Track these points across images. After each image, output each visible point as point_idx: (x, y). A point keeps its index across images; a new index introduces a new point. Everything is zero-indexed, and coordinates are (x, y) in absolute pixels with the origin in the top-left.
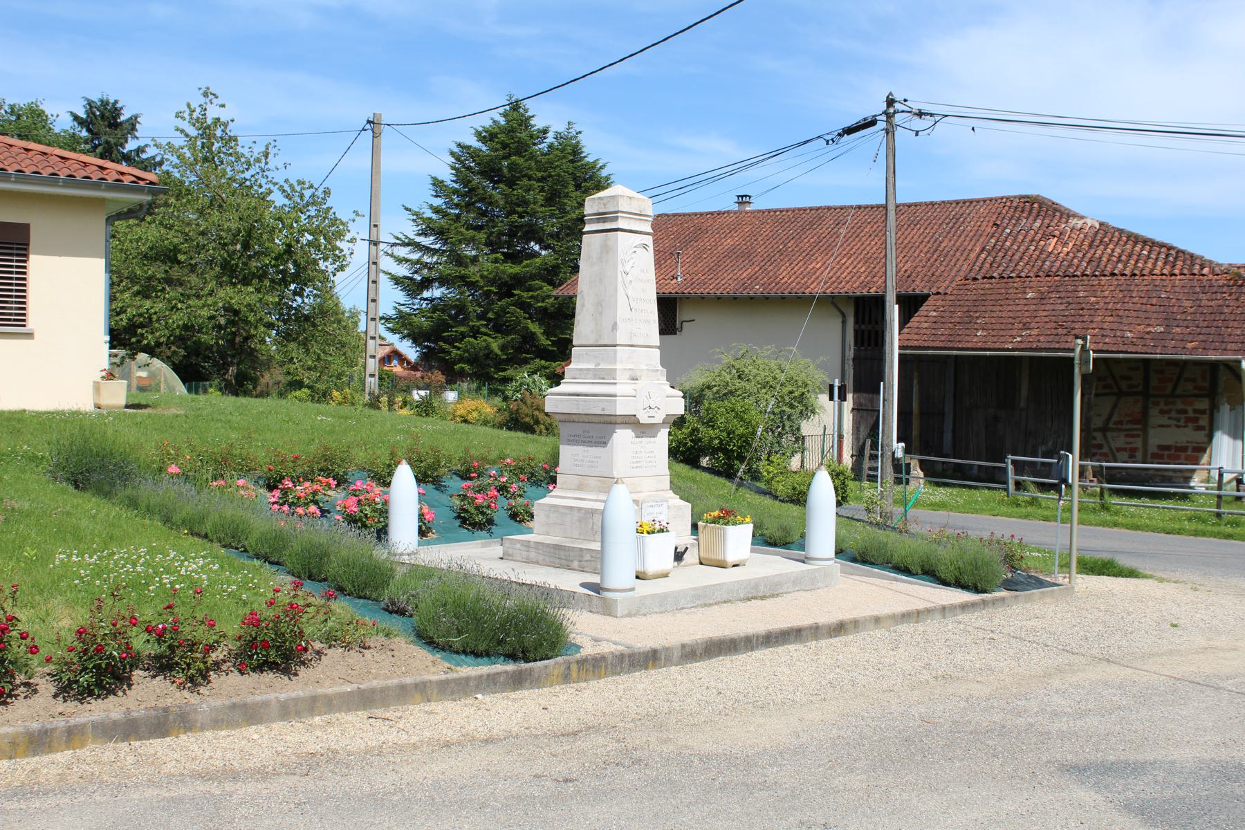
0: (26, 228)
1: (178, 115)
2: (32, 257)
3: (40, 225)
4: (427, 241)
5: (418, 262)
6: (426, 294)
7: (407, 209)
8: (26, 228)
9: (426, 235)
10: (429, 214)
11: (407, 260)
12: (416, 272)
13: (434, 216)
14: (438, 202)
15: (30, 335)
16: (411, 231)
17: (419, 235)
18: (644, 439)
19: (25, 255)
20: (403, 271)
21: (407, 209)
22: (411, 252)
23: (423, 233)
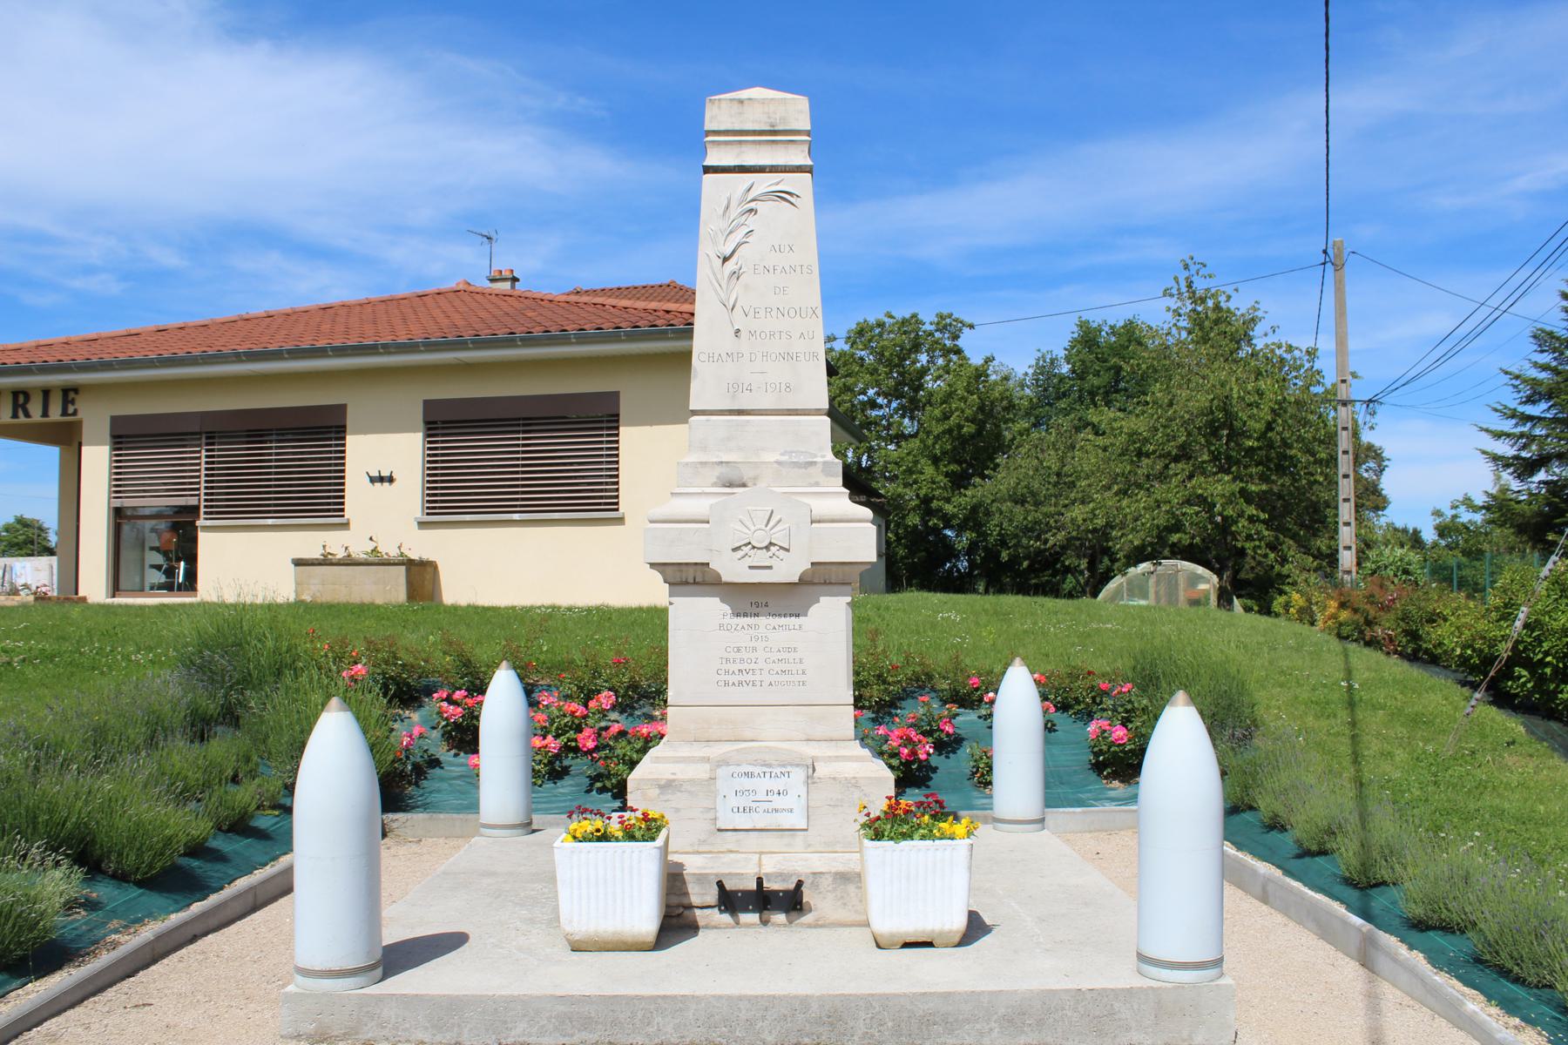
0: (616, 394)
1: (1167, 293)
2: (621, 429)
3: (631, 391)
4: (1531, 410)
5: (1522, 435)
6: (1542, 475)
7: (1506, 373)
8: (616, 394)
9: (1534, 402)
10: (1534, 373)
11: (1508, 435)
12: (1524, 447)
13: (1543, 375)
14: (1545, 358)
15: (620, 520)
16: (1512, 400)
17: (1525, 403)
18: (762, 621)
19: (617, 428)
20: (1505, 449)
21: (1506, 373)
22: (1516, 425)
23: (1530, 400)
